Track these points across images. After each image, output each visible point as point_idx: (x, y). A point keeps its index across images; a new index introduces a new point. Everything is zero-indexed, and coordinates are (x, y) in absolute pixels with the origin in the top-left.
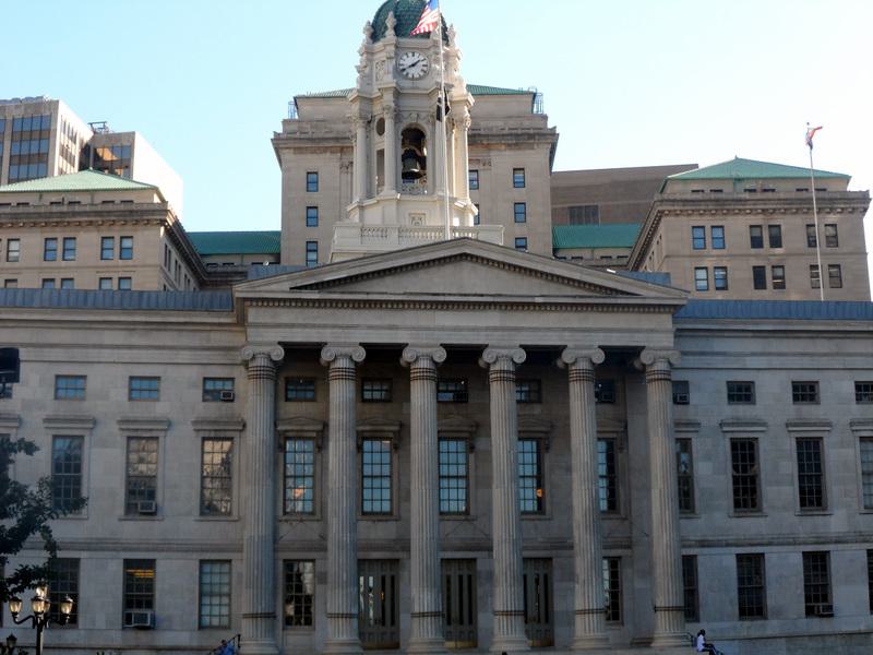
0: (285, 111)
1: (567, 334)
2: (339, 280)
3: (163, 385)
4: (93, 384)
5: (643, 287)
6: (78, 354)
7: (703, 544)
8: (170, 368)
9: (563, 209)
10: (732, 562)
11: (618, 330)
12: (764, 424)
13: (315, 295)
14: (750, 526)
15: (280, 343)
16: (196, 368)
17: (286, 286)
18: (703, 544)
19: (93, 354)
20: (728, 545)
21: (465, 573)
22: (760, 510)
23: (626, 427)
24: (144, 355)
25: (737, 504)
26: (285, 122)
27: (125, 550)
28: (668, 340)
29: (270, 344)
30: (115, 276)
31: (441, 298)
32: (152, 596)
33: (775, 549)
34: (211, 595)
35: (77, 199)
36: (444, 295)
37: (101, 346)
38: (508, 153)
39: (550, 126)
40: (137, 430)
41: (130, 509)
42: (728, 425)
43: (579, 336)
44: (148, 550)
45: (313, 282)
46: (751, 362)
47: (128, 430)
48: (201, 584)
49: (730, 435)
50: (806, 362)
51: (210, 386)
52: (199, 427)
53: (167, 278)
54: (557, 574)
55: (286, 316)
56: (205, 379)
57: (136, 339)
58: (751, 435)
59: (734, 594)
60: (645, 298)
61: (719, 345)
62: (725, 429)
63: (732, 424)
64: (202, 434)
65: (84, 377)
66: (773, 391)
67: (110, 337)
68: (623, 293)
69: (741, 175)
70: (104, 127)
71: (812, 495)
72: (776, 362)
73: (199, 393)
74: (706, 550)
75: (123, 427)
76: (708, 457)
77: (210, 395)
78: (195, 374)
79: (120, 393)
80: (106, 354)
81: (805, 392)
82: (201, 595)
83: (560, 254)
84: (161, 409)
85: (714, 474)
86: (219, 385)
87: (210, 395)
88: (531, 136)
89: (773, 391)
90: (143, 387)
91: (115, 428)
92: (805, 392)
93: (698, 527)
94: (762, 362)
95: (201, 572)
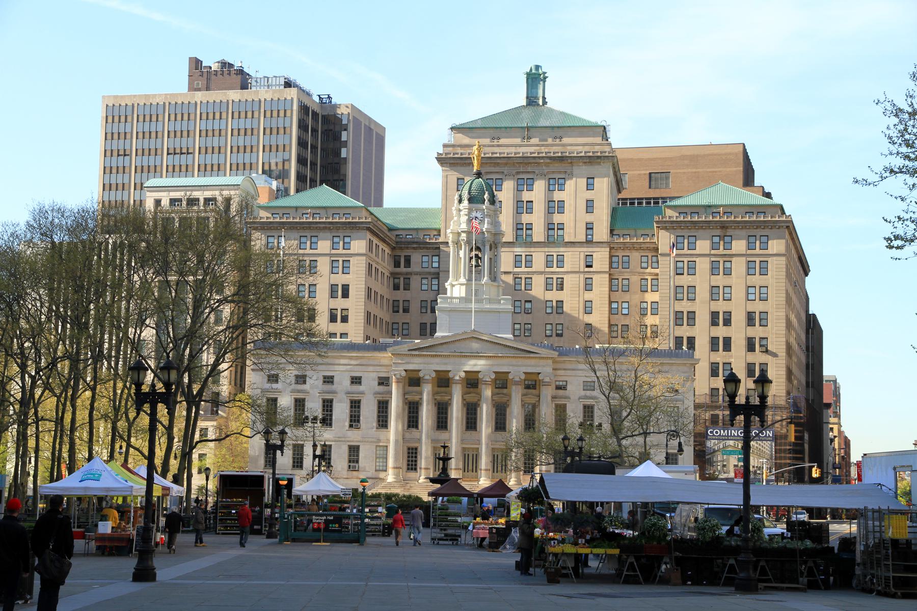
0: (447, 137)
4: (335, 379)
9: (645, 174)
11: (531, 366)
16: (375, 373)
26: (445, 146)
28: (549, 370)
30: (341, 259)
34: (379, 458)
35: (318, 212)
37: (340, 365)
38: (584, 167)
41: (351, 426)
43: (516, 368)
53: (370, 258)
55: (407, 359)
57: (353, 362)
67: (343, 361)
68: (533, 352)
70: (329, 97)
77: (380, 384)
79: (347, 382)
82: (376, 458)
83: (615, 233)
87: (380, 384)
88: (598, 157)
90: (356, 380)
91: (345, 396)
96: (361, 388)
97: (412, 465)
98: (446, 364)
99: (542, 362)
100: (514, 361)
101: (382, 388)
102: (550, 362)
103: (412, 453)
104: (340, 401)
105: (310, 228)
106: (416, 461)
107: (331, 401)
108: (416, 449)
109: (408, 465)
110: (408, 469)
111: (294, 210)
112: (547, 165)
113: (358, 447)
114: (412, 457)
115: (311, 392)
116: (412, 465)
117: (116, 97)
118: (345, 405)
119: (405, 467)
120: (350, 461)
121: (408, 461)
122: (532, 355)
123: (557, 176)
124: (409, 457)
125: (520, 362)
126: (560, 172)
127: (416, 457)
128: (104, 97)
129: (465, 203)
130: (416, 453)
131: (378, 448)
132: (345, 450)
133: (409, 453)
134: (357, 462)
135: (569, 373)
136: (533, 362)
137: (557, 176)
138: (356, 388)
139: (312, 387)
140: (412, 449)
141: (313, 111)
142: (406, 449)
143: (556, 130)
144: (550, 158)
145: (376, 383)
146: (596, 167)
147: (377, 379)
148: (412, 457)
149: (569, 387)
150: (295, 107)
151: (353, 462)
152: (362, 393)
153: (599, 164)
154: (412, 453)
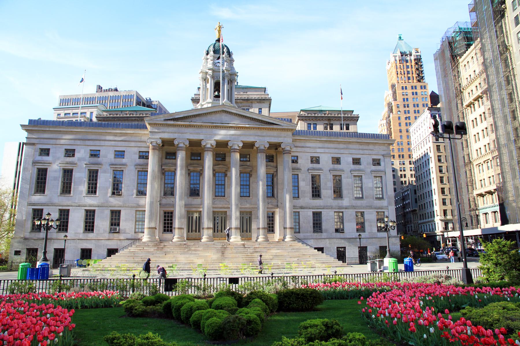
1: (256, 137)
2: (181, 118)
3: (125, 153)
5: (282, 123)
6: (97, 143)
7: (302, 208)
8: (128, 148)
10: (311, 214)
11: (273, 137)
12: (322, 170)
13: (172, 122)
14: (317, 202)
15: (160, 138)
16: (136, 148)
17: (163, 119)
18: (302, 208)
19: (102, 143)
20: (310, 209)
21: (223, 216)
22: (321, 198)
23: (277, 170)
24: (120, 144)
25: (313, 196)
26: (195, 95)
27: (110, 207)
29: (157, 138)
31: (215, 124)
32: (119, 222)
33: (325, 210)
34: (139, 221)
36: (215, 123)
39: (269, 97)
40: (116, 168)
41: (113, 193)
42: (310, 170)
43: (260, 138)
44: (118, 207)
45: (171, 118)
46: (319, 150)
47: (113, 168)
48: (136, 218)
49: (311, 173)
50: (336, 151)
51: (141, 154)
52: (137, 167)
54: (253, 217)
55: (163, 129)
56: (140, 152)
58: (318, 174)
59: (312, 224)
60: (283, 126)
61: (308, 144)
62: (309, 171)
63: (312, 170)
64: (138, 169)
65: (99, 151)
66: (326, 160)
69: (322, 109)
70: (150, 99)
71: (338, 192)
72: (327, 150)
73: (137, 156)
74: (302, 210)
75: (112, 167)
76: (304, 180)
77: (141, 157)
78: (136, 150)
79: (111, 156)
80: (107, 143)
81: (337, 161)
84: (124, 161)
85: (305, 186)
86: (144, 154)
87: (141, 157)
88: (264, 100)
89: (326, 160)
92: (337, 161)
93: (301, 202)
94: (322, 150)
95: (136, 214)
96: (124, 161)
97: (168, 227)
98: (198, 134)
99: (283, 133)
100: (259, 132)
101: (142, 161)
102: (290, 133)
103: (168, 217)
104: (105, 172)
105: (128, 120)
106: (171, 224)
107: (97, 171)
108: (172, 213)
109: (165, 227)
110: (165, 231)
111: (121, 112)
112: (241, 103)
113: (119, 212)
114: (168, 220)
115: (78, 163)
116: (168, 227)
117: (64, 96)
118: (109, 174)
119: (162, 229)
120: (112, 225)
121: (165, 224)
122: (275, 127)
123: (245, 108)
124: (165, 220)
125: (265, 133)
126: (247, 106)
127: (171, 220)
128: (60, 96)
129: (211, 53)
130: (172, 217)
131: (138, 213)
132: (108, 213)
133: (165, 216)
134: (119, 225)
135: (299, 149)
136: (275, 133)
137: (245, 108)
138: (119, 161)
139: (79, 159)
140: (168, 213)
141: (143, 102)
142: (162, 213)
143: (244, 89)
144: (243, 100)
145: (137, 156)
146: (263, 104)
147: (138, 153)
148: (168, 220)
149: (299, 161)
150: (135, 98)
151: (115, 225)
152: (125, 165)
153: (264, 103)
154: (168, 217)
